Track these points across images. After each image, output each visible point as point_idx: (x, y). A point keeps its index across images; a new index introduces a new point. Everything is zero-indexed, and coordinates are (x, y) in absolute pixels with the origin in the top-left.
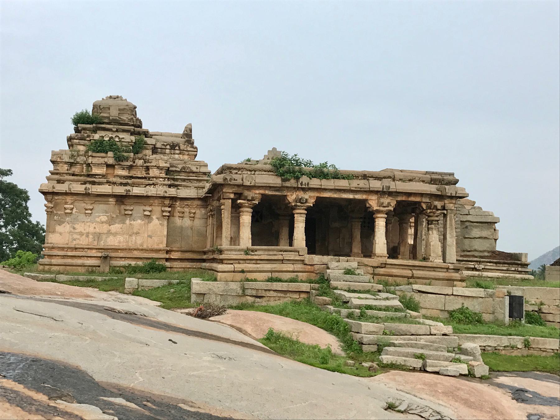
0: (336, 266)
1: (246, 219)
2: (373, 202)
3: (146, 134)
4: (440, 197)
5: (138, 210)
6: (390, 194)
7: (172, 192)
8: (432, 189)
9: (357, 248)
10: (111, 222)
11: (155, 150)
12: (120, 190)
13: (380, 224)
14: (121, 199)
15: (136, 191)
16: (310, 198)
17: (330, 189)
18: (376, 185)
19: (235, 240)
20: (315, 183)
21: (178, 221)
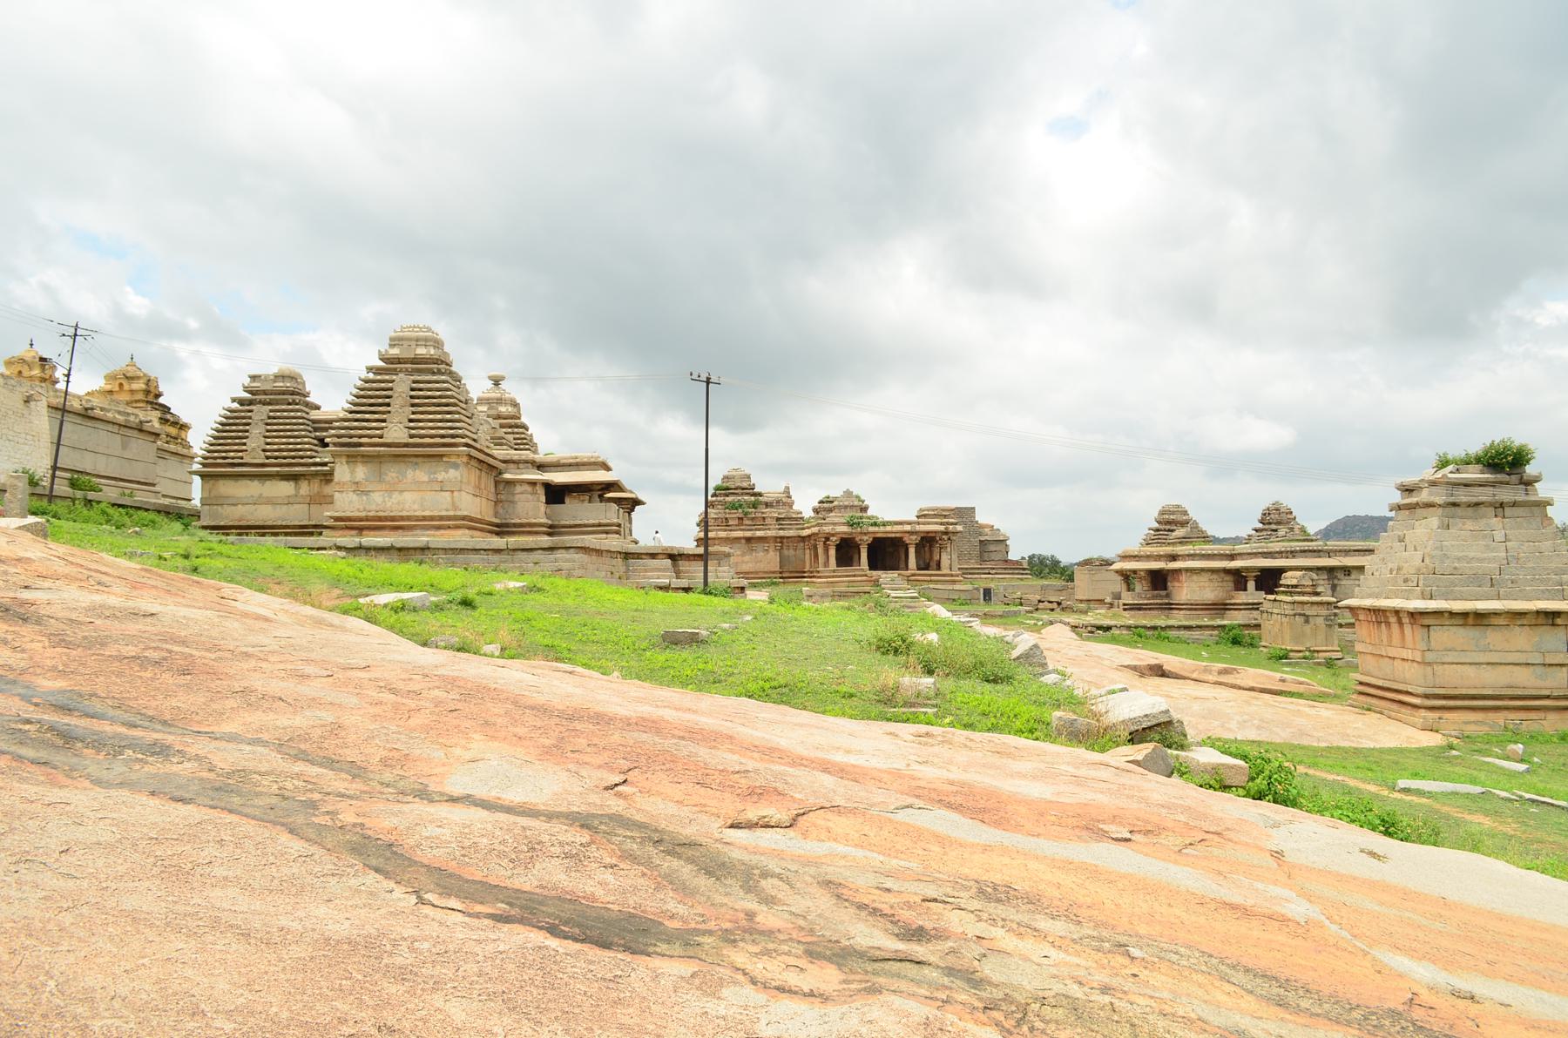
0: (885, 576)
1: (832, 552)
2: (907, 539)
3: (760, 495)
4: (946, 533)
5: (760, 546)
6: (916, 533)
7: (782, 533)
8: (942, 528)
9: (902, 565)
10: (743, 555)
11: (767, 505)
12: (748, 534)
13: (912, 551)
14: (748, 540)
15: (759, 534)
16: (868, 539)
17: (880, 531)
18: (908, 528)
19: (826, 564)
20: (871, 529)
21: (786, 552)
